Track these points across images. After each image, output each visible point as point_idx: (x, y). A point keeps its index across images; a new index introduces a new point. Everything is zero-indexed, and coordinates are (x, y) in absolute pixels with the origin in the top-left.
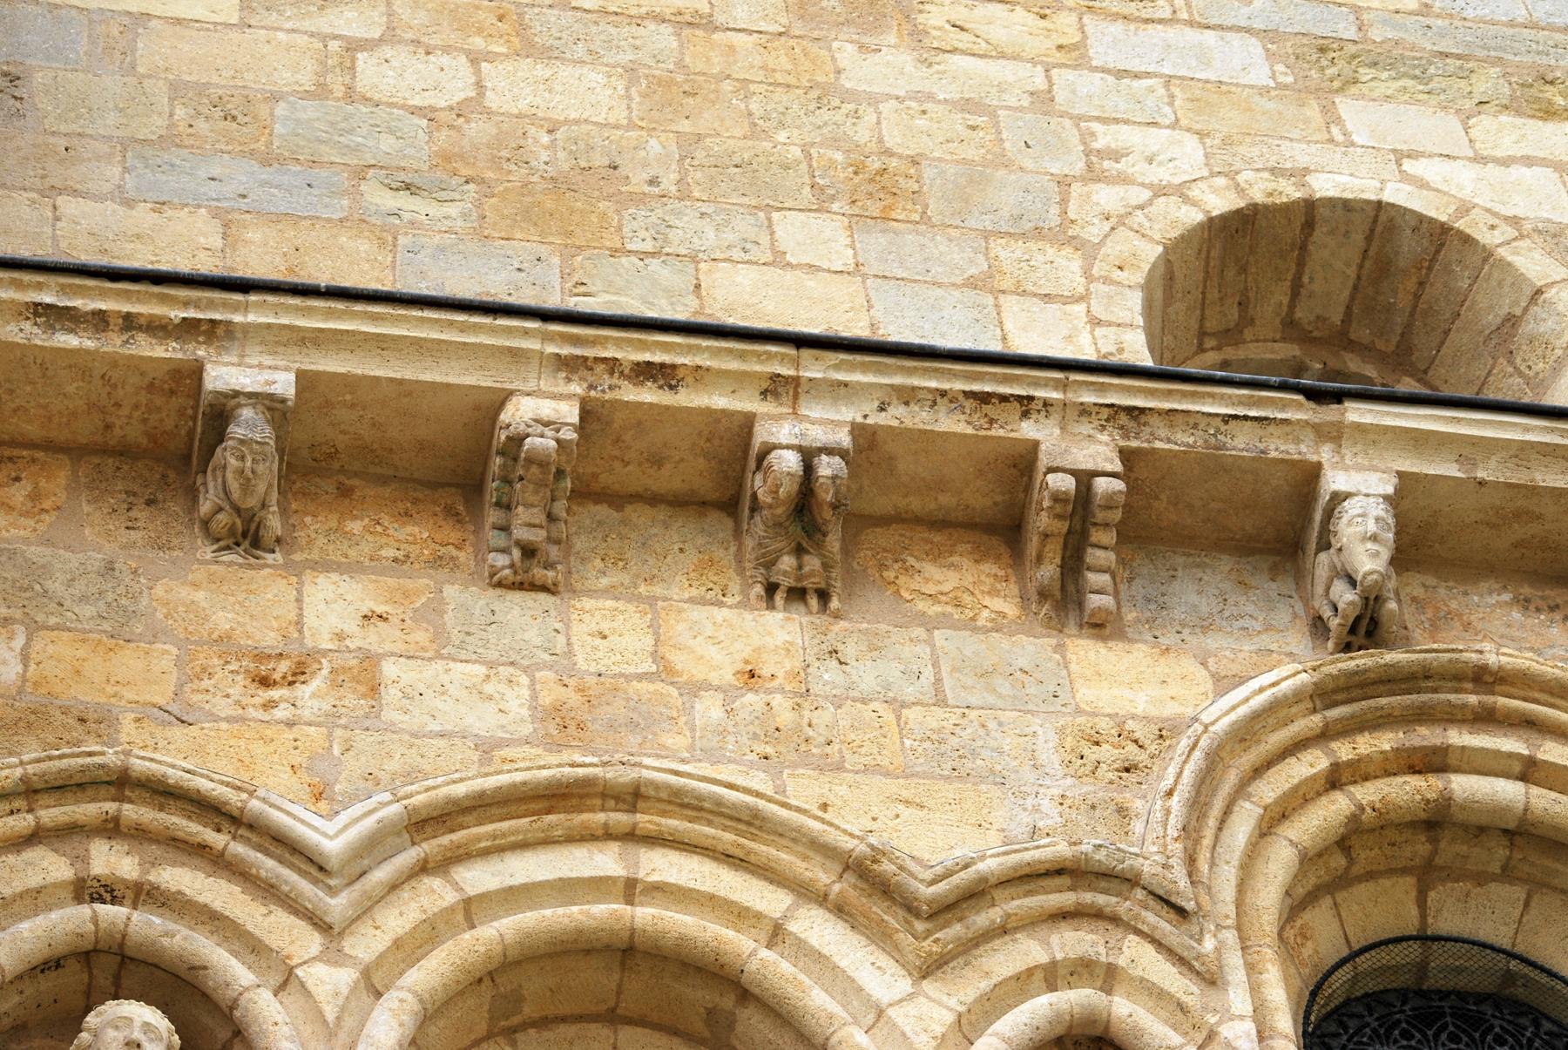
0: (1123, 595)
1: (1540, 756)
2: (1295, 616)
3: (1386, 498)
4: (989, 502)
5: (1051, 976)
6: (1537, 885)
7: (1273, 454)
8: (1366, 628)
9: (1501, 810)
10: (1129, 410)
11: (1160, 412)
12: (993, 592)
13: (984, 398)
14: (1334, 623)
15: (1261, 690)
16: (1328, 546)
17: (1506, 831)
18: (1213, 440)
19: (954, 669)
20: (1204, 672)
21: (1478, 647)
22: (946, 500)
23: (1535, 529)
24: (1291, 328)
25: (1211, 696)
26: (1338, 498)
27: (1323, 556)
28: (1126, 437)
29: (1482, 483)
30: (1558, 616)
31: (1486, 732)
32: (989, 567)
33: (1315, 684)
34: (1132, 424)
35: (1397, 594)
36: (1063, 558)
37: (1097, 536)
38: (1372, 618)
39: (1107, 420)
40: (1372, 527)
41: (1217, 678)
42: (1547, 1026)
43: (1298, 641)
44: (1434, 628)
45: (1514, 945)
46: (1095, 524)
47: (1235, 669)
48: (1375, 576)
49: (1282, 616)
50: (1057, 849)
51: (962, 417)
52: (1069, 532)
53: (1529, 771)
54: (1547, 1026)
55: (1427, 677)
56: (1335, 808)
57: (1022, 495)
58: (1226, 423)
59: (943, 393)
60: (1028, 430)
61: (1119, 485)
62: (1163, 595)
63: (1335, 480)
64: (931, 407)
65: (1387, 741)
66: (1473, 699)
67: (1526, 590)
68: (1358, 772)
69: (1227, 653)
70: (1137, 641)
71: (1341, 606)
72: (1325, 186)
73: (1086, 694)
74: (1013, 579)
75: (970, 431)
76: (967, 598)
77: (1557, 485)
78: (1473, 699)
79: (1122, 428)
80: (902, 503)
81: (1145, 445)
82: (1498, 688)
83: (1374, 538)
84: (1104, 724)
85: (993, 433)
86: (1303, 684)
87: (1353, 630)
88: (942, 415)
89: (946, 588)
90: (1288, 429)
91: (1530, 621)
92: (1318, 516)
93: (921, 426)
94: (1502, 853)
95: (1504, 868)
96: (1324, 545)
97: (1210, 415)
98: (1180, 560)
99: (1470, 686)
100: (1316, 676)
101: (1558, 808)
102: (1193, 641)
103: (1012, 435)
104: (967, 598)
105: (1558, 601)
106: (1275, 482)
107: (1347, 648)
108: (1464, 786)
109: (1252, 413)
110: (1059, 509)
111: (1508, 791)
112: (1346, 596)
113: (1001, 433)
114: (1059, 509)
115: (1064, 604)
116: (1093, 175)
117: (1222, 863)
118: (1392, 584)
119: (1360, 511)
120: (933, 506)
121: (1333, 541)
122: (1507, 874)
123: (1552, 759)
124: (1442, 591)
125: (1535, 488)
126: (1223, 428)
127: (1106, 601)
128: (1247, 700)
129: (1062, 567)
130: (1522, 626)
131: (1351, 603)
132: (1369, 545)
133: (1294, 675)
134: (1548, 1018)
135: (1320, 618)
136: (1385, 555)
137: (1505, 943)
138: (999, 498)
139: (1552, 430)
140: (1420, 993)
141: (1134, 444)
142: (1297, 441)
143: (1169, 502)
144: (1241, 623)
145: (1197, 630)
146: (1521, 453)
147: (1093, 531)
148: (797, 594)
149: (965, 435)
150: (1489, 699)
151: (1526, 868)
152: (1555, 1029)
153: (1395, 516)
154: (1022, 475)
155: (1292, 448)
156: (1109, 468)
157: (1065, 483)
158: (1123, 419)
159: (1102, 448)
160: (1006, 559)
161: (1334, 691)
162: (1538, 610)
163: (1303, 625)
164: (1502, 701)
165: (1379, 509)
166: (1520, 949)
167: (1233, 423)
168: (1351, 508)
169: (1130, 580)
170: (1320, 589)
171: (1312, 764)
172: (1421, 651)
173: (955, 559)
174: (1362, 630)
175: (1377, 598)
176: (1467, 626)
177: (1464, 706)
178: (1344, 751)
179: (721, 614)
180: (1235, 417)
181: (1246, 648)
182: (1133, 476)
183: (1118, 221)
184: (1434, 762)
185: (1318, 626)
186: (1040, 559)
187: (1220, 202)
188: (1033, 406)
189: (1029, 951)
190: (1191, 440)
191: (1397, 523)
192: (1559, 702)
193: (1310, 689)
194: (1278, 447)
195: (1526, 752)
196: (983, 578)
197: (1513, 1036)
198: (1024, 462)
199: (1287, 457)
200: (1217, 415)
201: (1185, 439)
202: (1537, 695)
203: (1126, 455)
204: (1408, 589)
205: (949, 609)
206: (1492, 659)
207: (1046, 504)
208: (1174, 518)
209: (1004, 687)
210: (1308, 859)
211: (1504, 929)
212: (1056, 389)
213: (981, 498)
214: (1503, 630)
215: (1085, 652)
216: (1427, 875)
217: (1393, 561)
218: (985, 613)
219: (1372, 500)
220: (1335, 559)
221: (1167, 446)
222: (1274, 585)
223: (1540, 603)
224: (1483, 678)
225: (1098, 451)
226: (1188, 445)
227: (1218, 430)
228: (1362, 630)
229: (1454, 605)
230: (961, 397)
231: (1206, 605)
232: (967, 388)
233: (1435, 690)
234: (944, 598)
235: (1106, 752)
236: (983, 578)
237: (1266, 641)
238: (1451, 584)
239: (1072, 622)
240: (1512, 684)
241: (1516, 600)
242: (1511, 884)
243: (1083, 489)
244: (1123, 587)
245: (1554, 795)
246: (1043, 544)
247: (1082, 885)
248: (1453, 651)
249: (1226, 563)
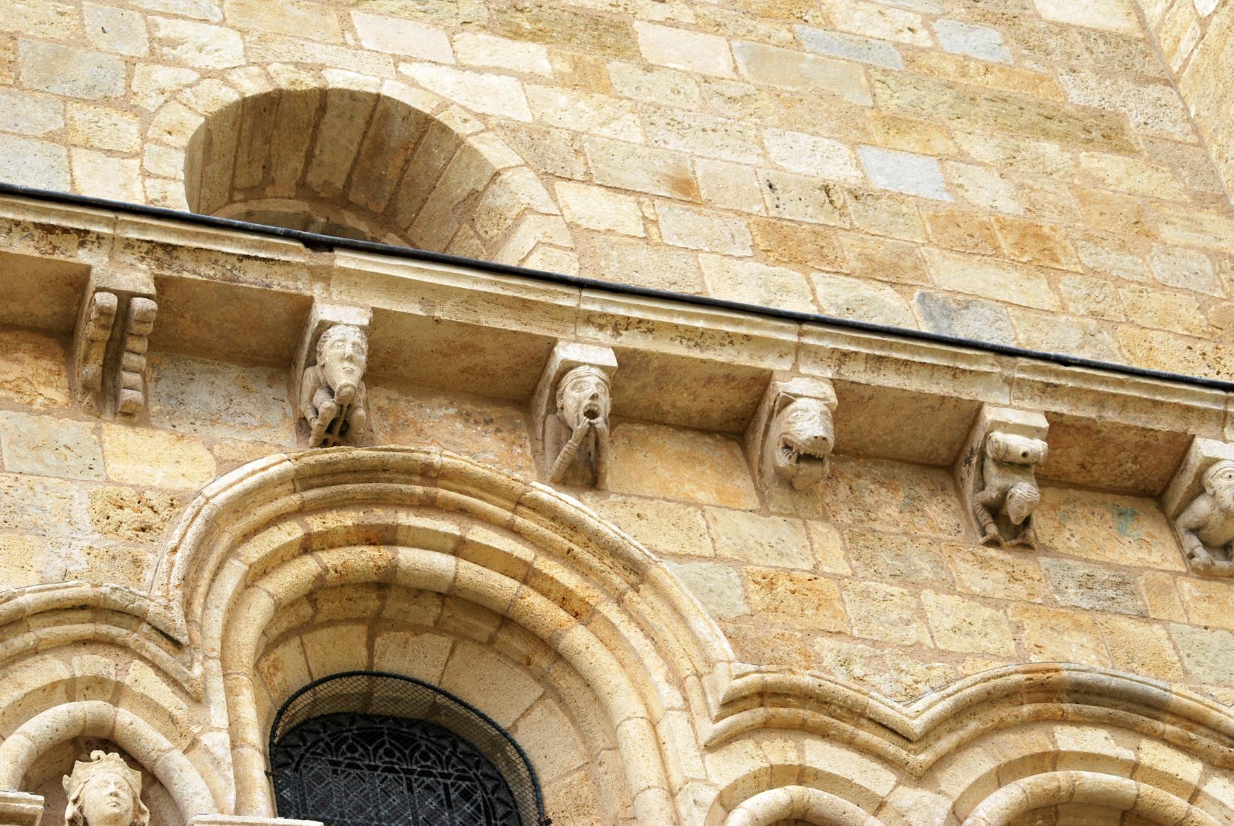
0: (150, 392)
1: (469, 537)
2: (285, 416)
3: (362, 328)
4: (49, 312)
5: (71, 689)
6: (460, 637)
7: (276, 288)
8: (340, 429)
9: (436, 577)
10: (165, 246)
11: (188, 249)
12: (47, 383)
13: (50, 229)
14: (315, 424)
15: (253, 473)
16: (315, 363)
17: (439, 594)
18: (229, 274)
19: (12, 442)
20: (210, 456)
21: (426, 449)
22: (15, 308)
23: (478, 359)
24: (303, 189)
25: (214, 475)
26: (324, 326)
27: (310, 370)
28: (161, 267)
29: (438, 321)
30: (491, 428)
31: (428, 516)
32: (46, 363)
33: (296, 470)
34: (167, 257)
35: (366, 403)
36: (105, 360)
37: (132, 344)
38: (345, 422)
39: (147, 253)
40: (349, 350)
41: (220, 461)
42: (462, 747)
43: (286, 436)
44: (394, 432)
45: (440, 683)
46: (131, 334)
47: (234, 455)
48: (349, 389)
49: (275, 415)
50: (82, 589)
51: (32, 243)
52: (111, 339)
53: (460, 548)
54: (462, 747)
55: (385, 470)
56: (306, 568)
57: (76, 308)
58: (241, 261)
59: (18, 223)
60: (83, 256)
61: (152, 305)
62: (183, 393)
63: (323, 312)
64: (8, 234)
65: (349, 519)
66: (419, 489)
67: (468, 407)
68: (326, 541)
69: (229, 442)
70: (159, 429)
71: (321, 410)
72: (336, 79)
73: (115, 468)
74: (64, 374)
75: (37, 254)
76: (26, 387)
77: (497, 326)
78: (419, 489)
79: (158, 260)
81: (175, 274)
82: (439, 482)
83: (350, 359)
84: (127, 493)
85: (55, 257)
86: (287, 471)
87: (330, 430)
88: (15, 241)
89: (10, 377)
90: (289, 269)
91: (469, 431)
92: (308, 339)
94: (435, 610)
95: (436, 623)
96: (312, 362)
97: (228, 254)
98: (198, 366)
99: (418, 479)
100: (297, 465)
101: (480, 578)
102: (203, 431)
103: (70, 260)
104: (26, 387)
105: (493, 416)
106: (276, 311)
107: (324, 443)
108: (409, 557)
109: (262, 255)
110: (103, 320)
111: (442, 563)
112: (325, 403)
113: (62, 257)
114: (103, 320)
115: (103, 395)
116: (154, 58)
117: (213, 608)
118: (362, 396)
119: (341, 337)
121: (318, 359)
122: (438, 627)
123: (478, 540)
124: (402, 403)
125: (480, 327)
126: (238, 265)
127: (136, 395)
128: (241, 480)
129: (103, 366)
130: (463, 435)
131: (329, 409)
132: (346, 364)
133: (280, 462)
134: (463, 741)
135: (305, 419)
136: (359, 372)
137: (434, 681)
138: (57, 309)
139: (496, 283)
140: (367, 717)
141: (167, 273)
142: (296, 279)
143: (192, 321)
144: (242, 419)
145: (207, 423)
146: (471, 299)
147: (129, 340)
149: (33, 258)
150: (432, 490)
151: (453, 623)
152: (468, 750)
153: (369, 342)
154: (77, 292)
155: (291, 284)
156: (145, 291)
157: (110, 301)
158: (159, 253)
159: (140, 275)
160: (60, 357)
161: (311, 477)
162: (476, 422)
163: (291, 424)
164: (442, 492)
165: (356, 337)
166: (444, 686)
167: (246, 262)
168: (334, 334)
169: (157, 380)
170: (305, 397)
171: (290, 532)
172: (381, 450)
173: (19, 355)
174: (337, 429)
175: (349, 406)
176: (420, 432)
177: (412, 494)
178: (316, 524)
180: (248, 257)
181: (244, 439)
182: (164, 298)
183: (171, 96)
184: (386, 537)
185: (303, 425)
186: (86, 359)
187: (253, 86)
188: (88, 238)
189: (54, 669)
190: (212, 273)
191: (370, 348)
192: (486, 495)
193: (292, 474)
194: (280, 283)
195: (458, 533)
196: (40, 371)
197: (435, 753)
198: (78, 282)
199: (287, 291)
200: (234, 255)
201: (206, 272)
202: (469, 489)
203: (160, 282)
204: (376, 401)
205: (11, 394)
206: (436, 459)
207: (93, 316)
208: (195, 333)
209: (51, 459)
210: (281, 608)
211: (433, 669)
212: (107, 225)
213: (43, 308)
214: (447, 437)
215: (117, 434)
216: (375, 625)
217: (364, 378)
218: (40, 399)
219: (351, 329)
220: (319, 374)
221: (192, 277)
222: (270, 391)
223: (478, 417)
224: (429, 473)
225: (137, 277)
226: (209, 277)
227: (233, 267)
228: (337, 429)
229: (411, 415)
230: (31, 228)
231: (216, 403)
232: (37, 220)
233: (390, 481)
234: (8, 386)
235: (127, 515)
236: (40, 371)
237: (261, 434)
238: (410, 398)
239: (108, 410)
240: (451, 480)
241: (460, 414)
242: (441, 635)
243: (124, 306)
244: (151, 385)
245: (478, 568)
246: (89, 348)
247: (100, 618)
248: (407, 451)
249: (234, 371)
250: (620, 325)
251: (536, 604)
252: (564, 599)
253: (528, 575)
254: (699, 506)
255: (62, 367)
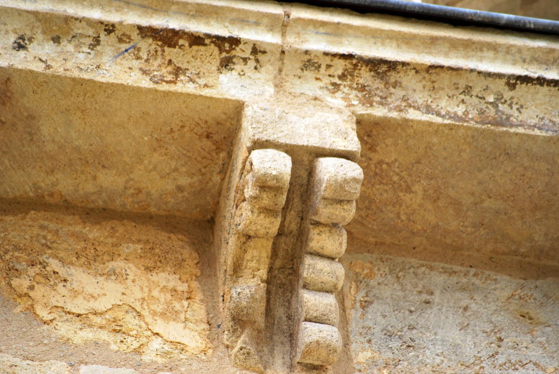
0: (353, 326)
4: (170, 187)
10: (375, 65)
11: (417, 69)
12: (169, 314)
13: (168, 38)
18: (492, 112)
22: (110, 180)
28: (368, 101)
32: (165, 278)
34: (376, 84)
36: (270, 270)
37: (320, 240)
39: (342, 77)
46: (317, 224)
51: (136, 64)
52: (280, 233)
57: (217, 178)
58: (512, 87)
59: (110, 28)
60: (229, 86)
61: (353, 170)
62: (411, 328)
64: (92, 47)
74: (199, 296)
75: (145, 83)
76: (131, 322)
79: (363, 88)
80: (45, 182)
81: (394, 115)
88: (106, 60)
89: (101, 305)
93: (76, 74)
97: (489, 75)
98: (439, 279)
103: (206, 92)
104: (131, 322)
110: (266, 200)
113: (190, 88)
114: (266, 200)
120: (90, 187)
126: (508, 94)
127: (329, 334)
129: (268, 282)
138: (184, 181)
141: (379, 112)
143: (426, 196)
147: (314, 233)
149: (139, 90)
154: (218, 149)
156: (341, 145)
157: (279, 165)
158: (365, 76)
159: (332, 117)
160: (191, 266)
167: (522, 88)
169: (365, 305)
173: (118, 264)
180: (526, 80)
182: (376, 157)
186: (237, 270)
188: (238, 52)
190: (460, 110)
198: (221, 132)
200: (500, 76)
203: (367, 129)
205: (104, 336)
207: (249, 192)
208: (432, 219)
212: (271, 28)
218: (156, 344)
221: (426, 118)
225: (325, 120)
226: (455, 117)
227: (500, 98)
230: (135, 35)
232: (146, 21)
234: (98, 320)
236: (155, 293)
239: (278, 361)
243: (304, 174)
244: (354, 314)
246: (243, 249)
249: (504, 286)
255: (195, 284)
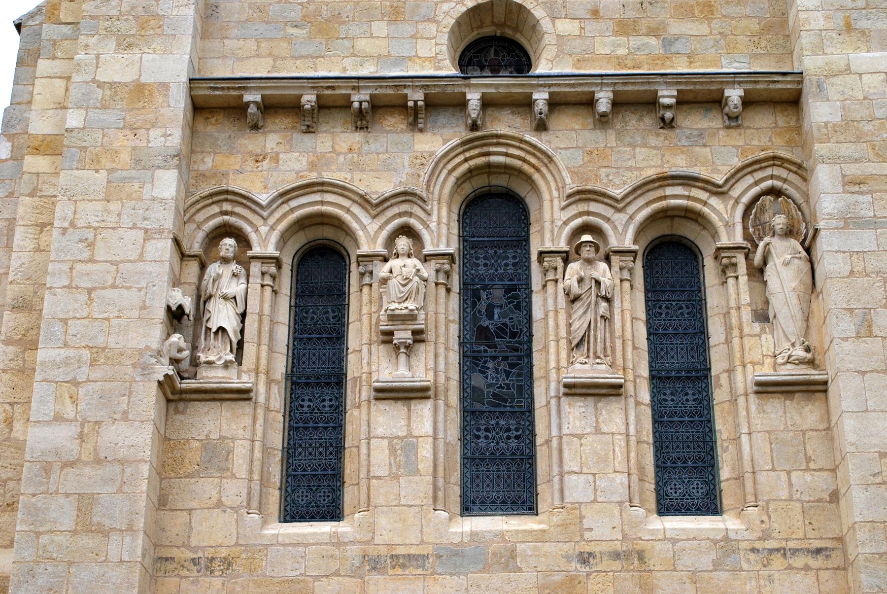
41: (444, 140)
53: (507, 155)
56: (466, 166)
60: (405, 91)
63: (468, 97)
65: (476, 151)
108: (494, 159)
122: (505, 173)
148: (362, 128)
171: (461, 158)
178: (468, 155)
179: (346, 135)
184: (488, 154)
206: (499, 132)
215: (418, 136)
224: (498, 136)
250: (550, 86)
251: (526, 167)
252: (533, 166)
253: (524, 160)
254: (575, 130)
